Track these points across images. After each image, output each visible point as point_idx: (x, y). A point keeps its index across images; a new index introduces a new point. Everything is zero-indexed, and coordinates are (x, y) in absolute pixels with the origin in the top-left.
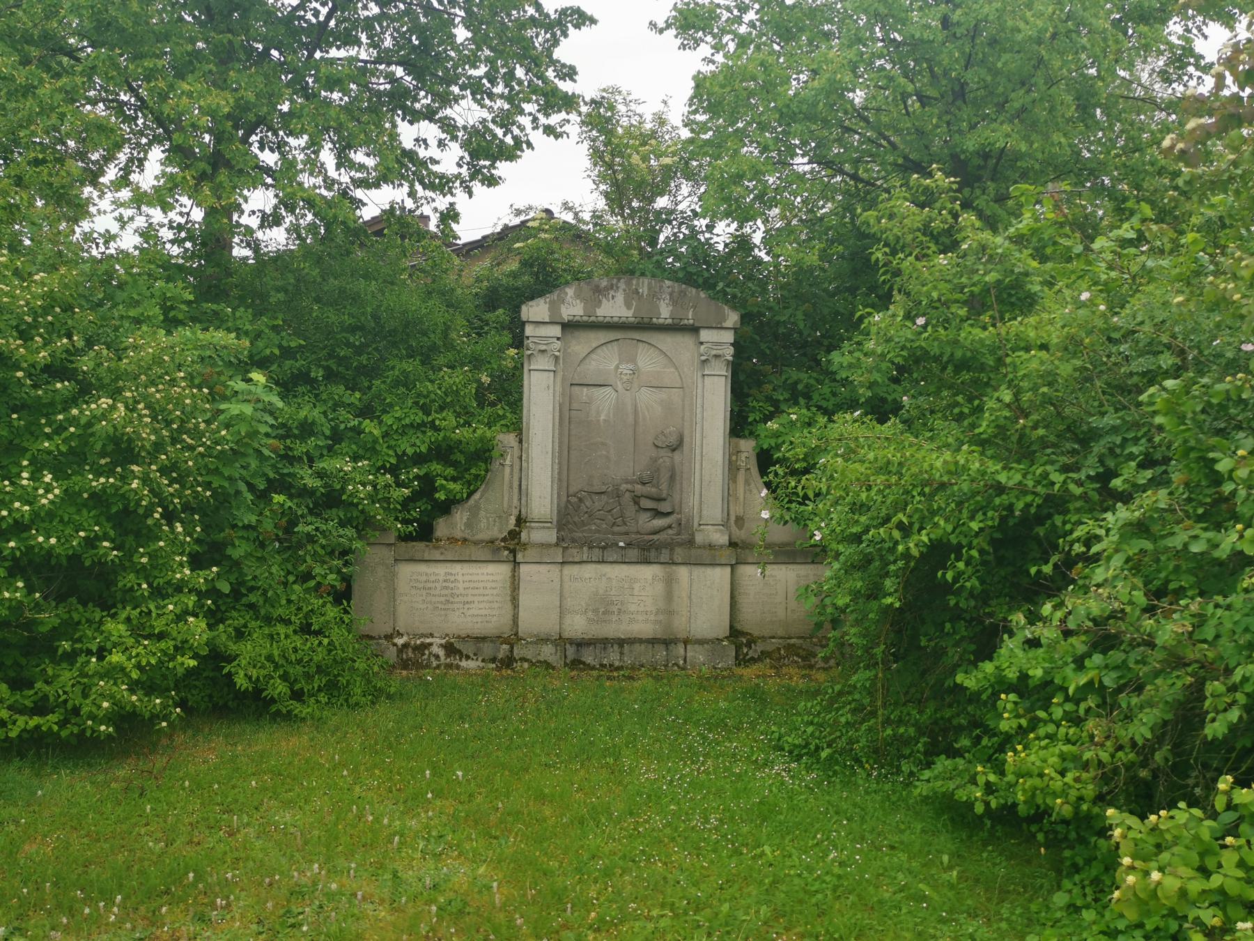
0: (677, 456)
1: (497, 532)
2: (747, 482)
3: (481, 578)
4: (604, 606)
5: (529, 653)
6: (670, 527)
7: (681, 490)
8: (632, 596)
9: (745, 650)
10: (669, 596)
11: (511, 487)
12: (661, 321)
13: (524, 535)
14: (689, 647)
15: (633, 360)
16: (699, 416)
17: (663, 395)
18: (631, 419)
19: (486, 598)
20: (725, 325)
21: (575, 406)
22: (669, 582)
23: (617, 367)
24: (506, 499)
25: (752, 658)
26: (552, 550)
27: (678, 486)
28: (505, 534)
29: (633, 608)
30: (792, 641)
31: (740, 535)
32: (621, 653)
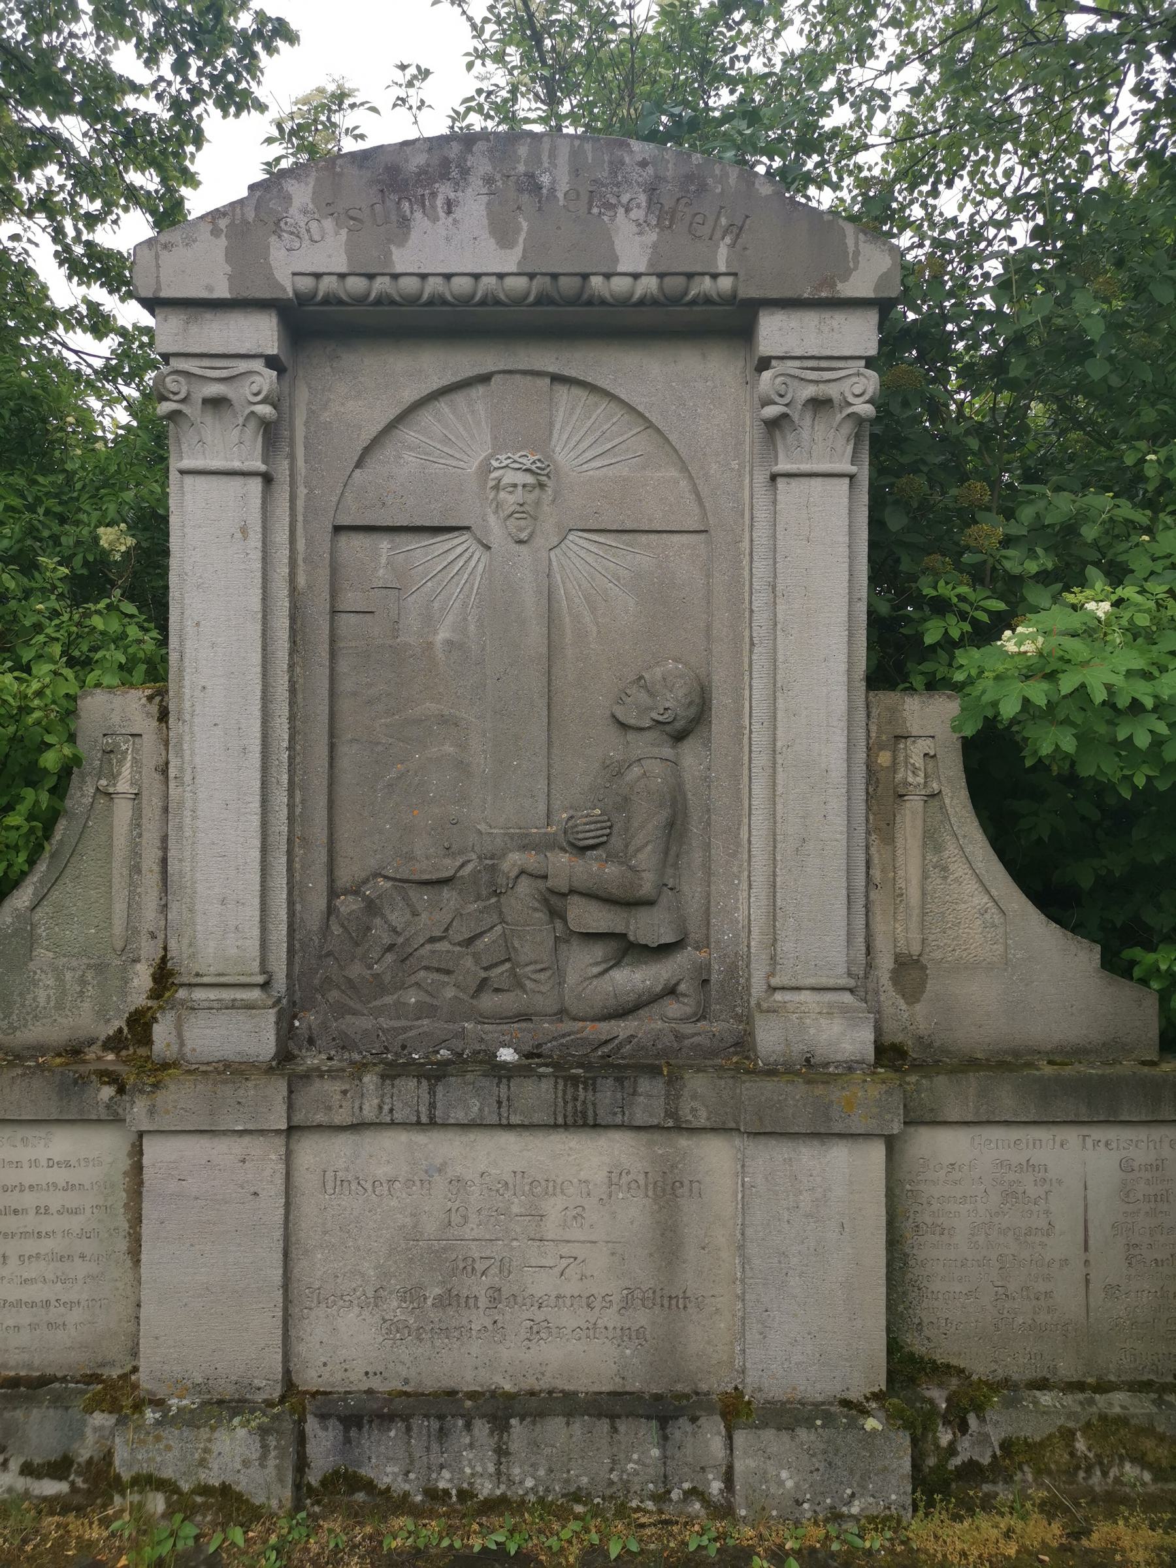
0: (690, 756)
1: (91, 1018)
2: (931, 840)
3: (29, 1176)
4: (440, 1278)
5: (169, 1456)
6: (671, 991)
7: (708, 872)
8: (530, 1244)
9: (945, 1437)
10: (668, 1242)
11: (136, 869)
12: (620, 285)
13: (162, 1033)
14: (740, 1437)
15: (541, 442)
16: (761, 618)
17: (639, 556)
18: (535, 635)
19: (46, 1246)
20: (848, 290)
21: (351, 599)
22: (669, 1190)
23: (486, 469)
24: (119, 908)
25: (972, 1471)
26: (249, 1091)
27: (697, 857)
28: (119, 1023)
29: (542, 1285)
30: (1118, 1402)
31: (911, 1019)
32: (501, 1452)
